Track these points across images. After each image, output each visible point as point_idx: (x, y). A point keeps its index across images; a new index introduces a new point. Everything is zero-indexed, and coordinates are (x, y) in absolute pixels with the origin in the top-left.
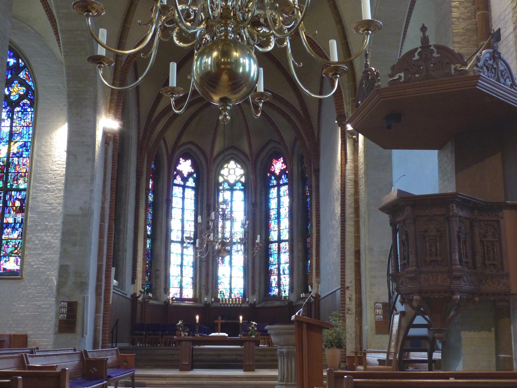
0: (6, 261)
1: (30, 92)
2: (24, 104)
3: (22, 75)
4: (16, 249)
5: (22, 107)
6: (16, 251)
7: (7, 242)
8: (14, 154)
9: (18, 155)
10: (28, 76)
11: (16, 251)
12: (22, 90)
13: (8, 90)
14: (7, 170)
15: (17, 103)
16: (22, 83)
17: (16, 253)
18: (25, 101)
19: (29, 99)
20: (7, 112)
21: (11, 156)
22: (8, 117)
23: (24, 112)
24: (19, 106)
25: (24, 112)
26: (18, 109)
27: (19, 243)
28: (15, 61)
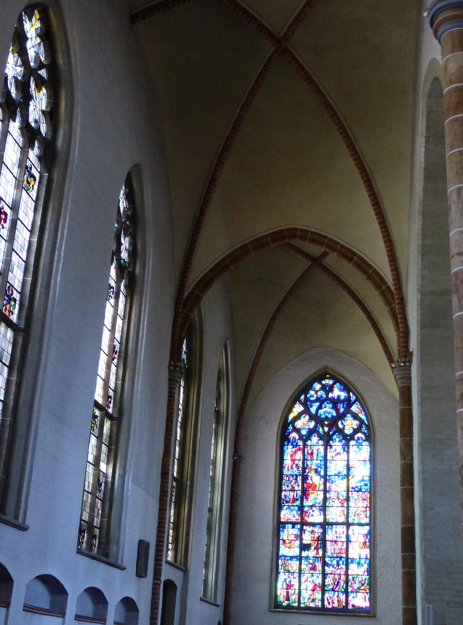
0: (354, 597)
1: (363, 426)
2: (358, 438)
3: (354, 408)
4: (363, 585)
5: (357, 441)
6: (363, 588)
7: (353, 578)
8: (353, 488)
9: (356, 489)
10: (360, 410)
11: (363, 588)
12: (356, 424)
13: (342, 423)
14: (348, 504)
15: (352, 437)
16: (355, 417)
17: (364, 589)
18: (360, 435)
19: (364, 433)
20: (343, 445)
21: (350, 490)
22: (344, 450)
23: (359, 445)
24: (353, 439)
25: (359, 445)
26: (352, 443)
27: (365, 579)
28: (346, 395)
